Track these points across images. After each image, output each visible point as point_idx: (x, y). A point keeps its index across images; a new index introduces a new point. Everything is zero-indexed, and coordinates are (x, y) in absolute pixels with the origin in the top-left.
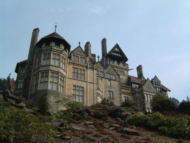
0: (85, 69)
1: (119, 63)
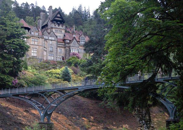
0: (38, 38)
1: (59, 25)
